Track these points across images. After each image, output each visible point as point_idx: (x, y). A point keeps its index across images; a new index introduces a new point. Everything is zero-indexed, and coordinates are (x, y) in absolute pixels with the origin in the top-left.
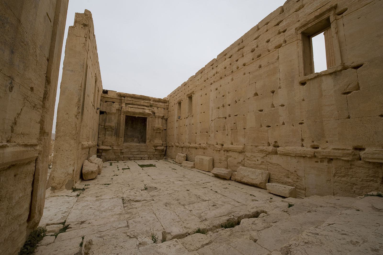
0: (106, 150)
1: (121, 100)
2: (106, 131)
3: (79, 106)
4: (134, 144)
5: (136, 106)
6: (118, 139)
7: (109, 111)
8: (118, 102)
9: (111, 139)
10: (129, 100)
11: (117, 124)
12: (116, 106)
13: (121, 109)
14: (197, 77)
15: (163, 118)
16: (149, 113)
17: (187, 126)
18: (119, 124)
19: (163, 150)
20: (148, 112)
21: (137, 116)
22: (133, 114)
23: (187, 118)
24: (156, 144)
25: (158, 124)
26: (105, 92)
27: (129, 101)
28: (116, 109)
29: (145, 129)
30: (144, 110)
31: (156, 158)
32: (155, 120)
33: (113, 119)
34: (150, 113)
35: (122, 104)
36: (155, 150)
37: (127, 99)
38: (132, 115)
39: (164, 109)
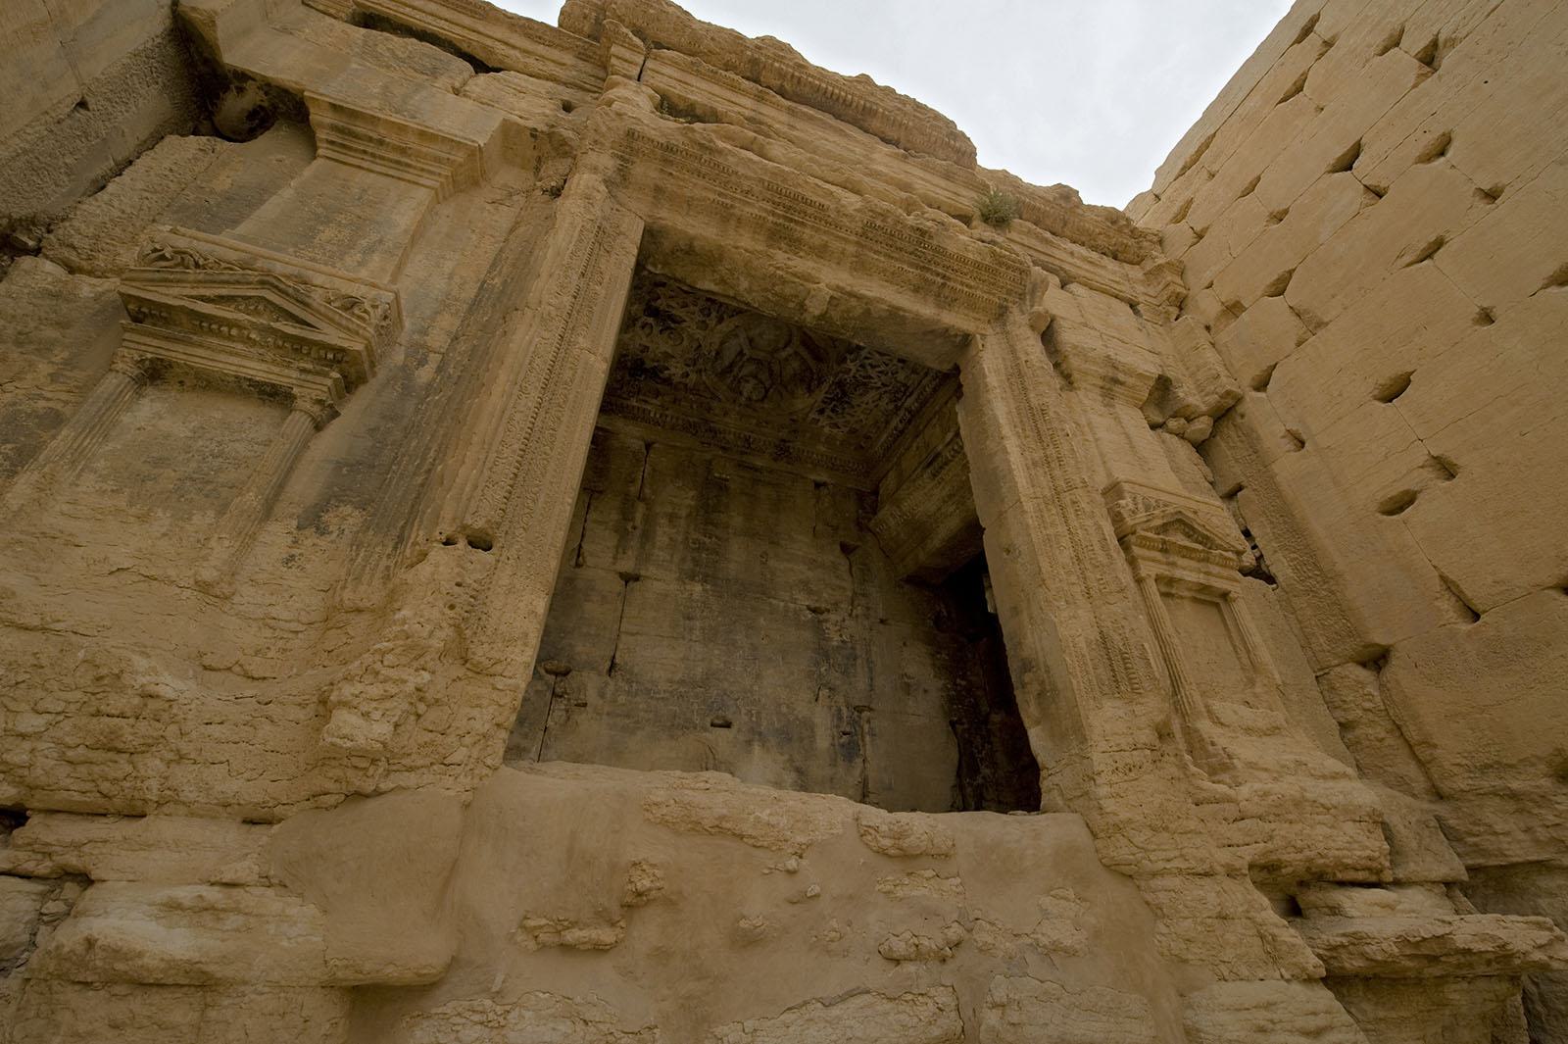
21: (826, 281)
22: (778, 235)
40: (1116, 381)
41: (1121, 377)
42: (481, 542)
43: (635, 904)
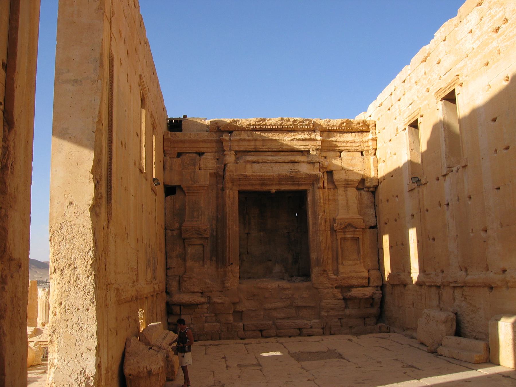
0: (191, 306)
1: (220, 142)
2: (185, 247)
3: (98, 177)
4: (274, 284)
5: (270, 158)
6: (222, 270)
7: (191, 182)
8: (214, 150)
9: (202, 273)
10: (245, 140)
11: (214, 222)
12: (209, 163)
13: (224, 170)
14: (464, 21)
15: (361, 187)
16: (310, 175)
17: (448, 205)
18: (220, 219)
19: (370, 301)
20: (308, 172)
21: (273, 189)
22: (262, 185)
23: (445, 176)
24: (344, 279)
25: (347, 207)
26: (175, 125)
27: (245, 144)
28: (208, 176)
29: (305, 231)
30: (296, 164)
31: (351, 327)
32: (334, 195)
33: (203, 206)
34: (316, 176)
35: (225, 155)
36: (342, 302)
37: (238, 138)
38: (257, 188)
39: (362, 155)
40: (347, 184)
41: (349, 183)
42: (232, 264)
43: (254, 296)
